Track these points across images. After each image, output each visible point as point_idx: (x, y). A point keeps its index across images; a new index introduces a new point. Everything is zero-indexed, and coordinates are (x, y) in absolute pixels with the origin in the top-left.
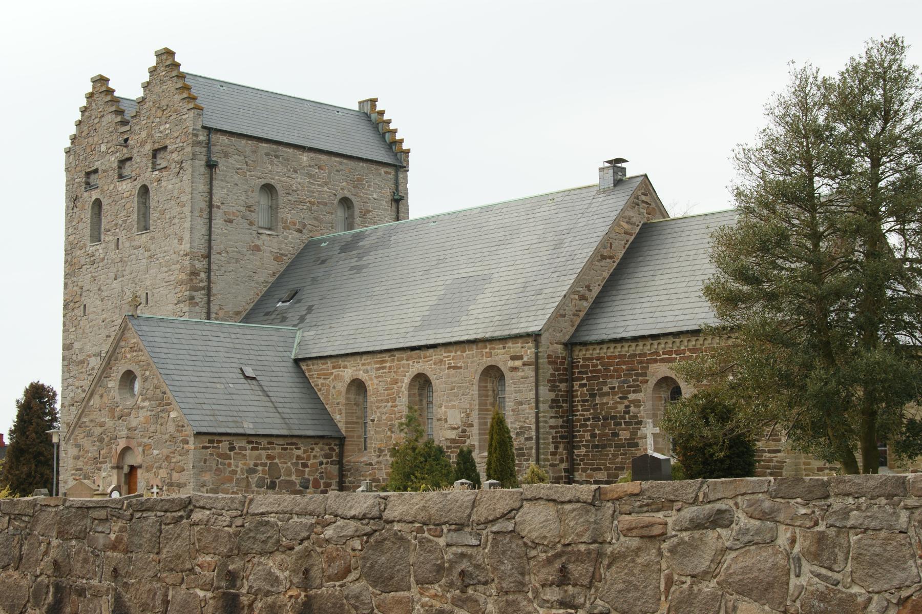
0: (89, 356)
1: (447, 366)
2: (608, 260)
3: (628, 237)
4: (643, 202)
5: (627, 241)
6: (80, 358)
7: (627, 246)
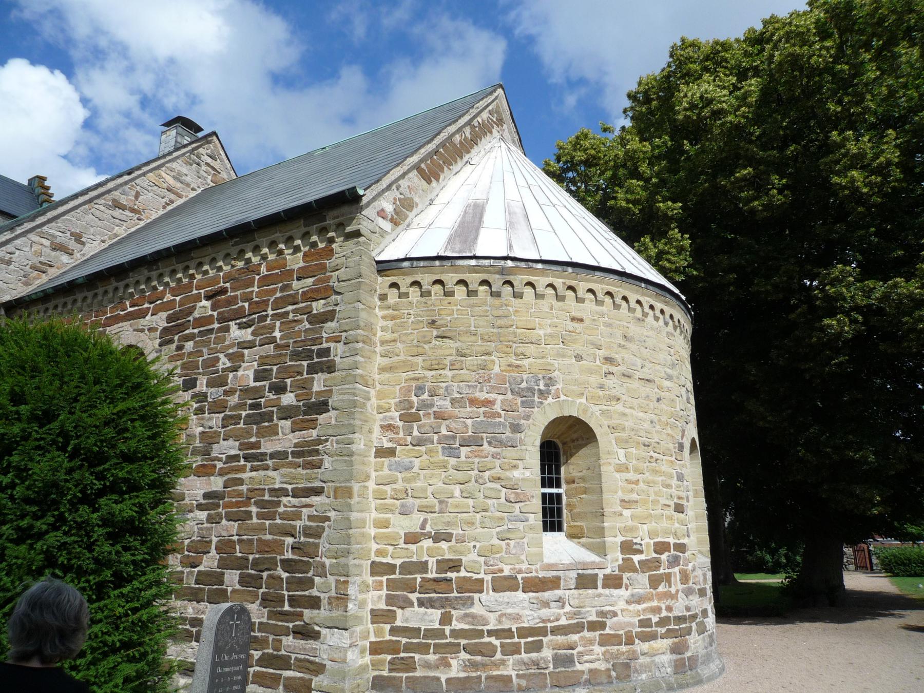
2: (127, 213)
3: (172, 197)
4: (207, 164)
5: (172, 202)
7: (169, 208)
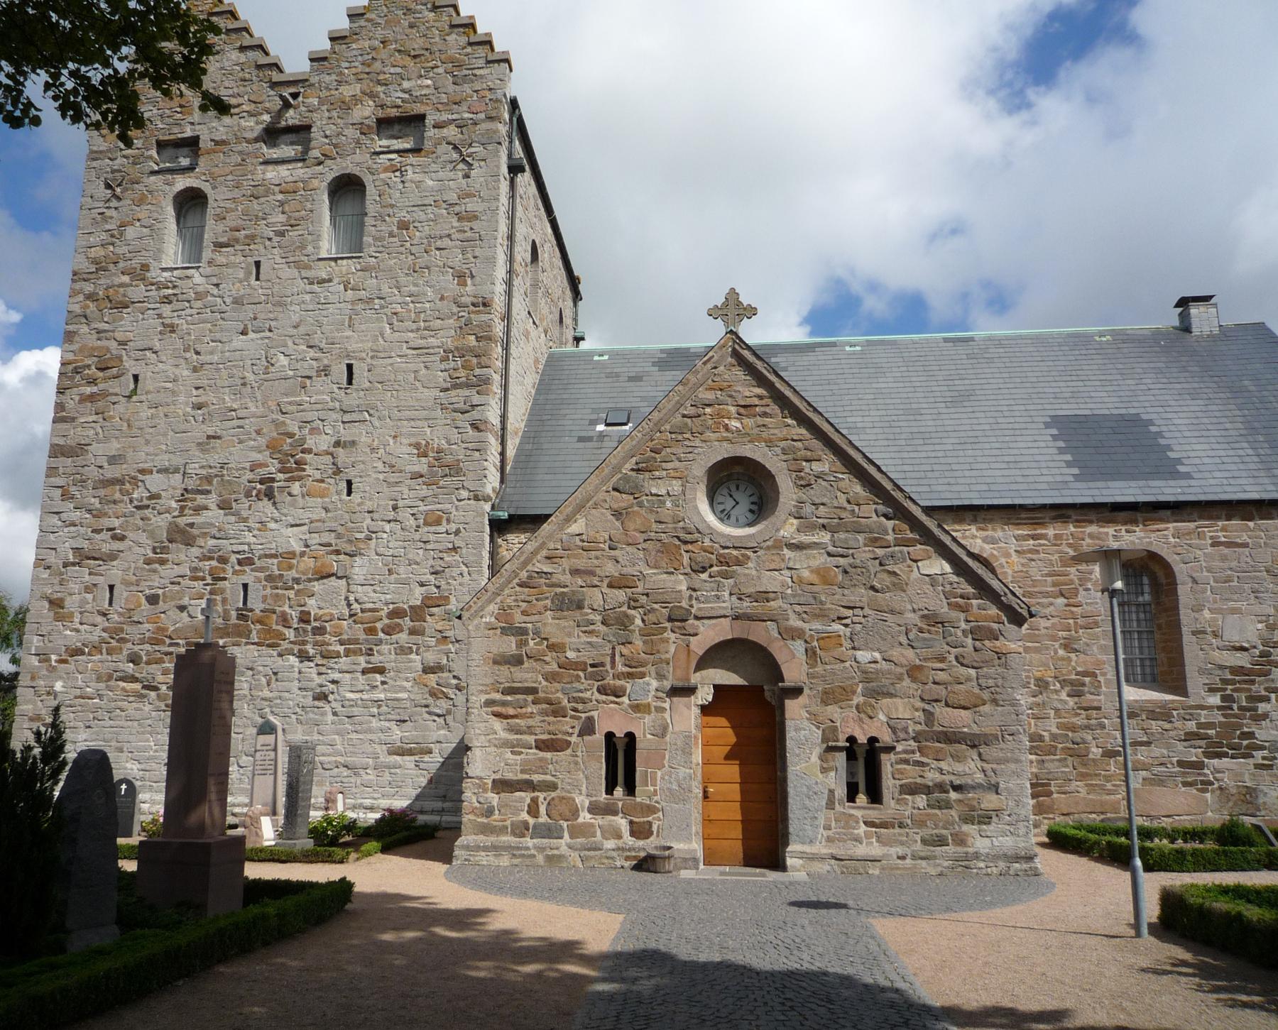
0: (142, 471)
1: (1210, 542)
6: (111, 472)
